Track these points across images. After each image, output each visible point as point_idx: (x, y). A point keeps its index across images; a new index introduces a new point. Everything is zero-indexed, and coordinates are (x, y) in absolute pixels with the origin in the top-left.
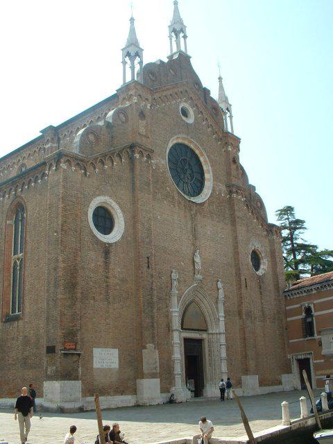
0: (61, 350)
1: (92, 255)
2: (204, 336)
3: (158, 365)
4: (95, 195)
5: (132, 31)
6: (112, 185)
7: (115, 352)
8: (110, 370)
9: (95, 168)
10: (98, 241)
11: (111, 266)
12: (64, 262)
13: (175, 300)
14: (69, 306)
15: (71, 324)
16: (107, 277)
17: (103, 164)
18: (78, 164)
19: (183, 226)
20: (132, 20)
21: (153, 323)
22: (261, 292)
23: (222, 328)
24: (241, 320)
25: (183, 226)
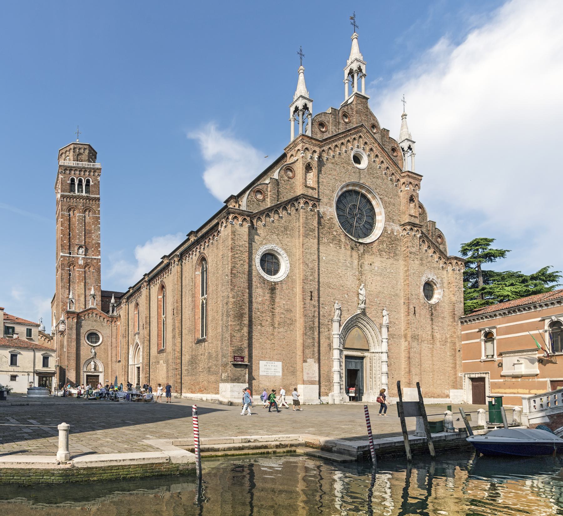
0: (232, 362)
1: (260, 291)
6: (278, 235)
10: (264, 280)
11: (277, 300)
12: (233, 297)
14: (238, 330)
15: (239, 343)
16: (273, 308)
19: (349, 265)
22: (432, 319)
24: (406, 342)
25: (349, 265)
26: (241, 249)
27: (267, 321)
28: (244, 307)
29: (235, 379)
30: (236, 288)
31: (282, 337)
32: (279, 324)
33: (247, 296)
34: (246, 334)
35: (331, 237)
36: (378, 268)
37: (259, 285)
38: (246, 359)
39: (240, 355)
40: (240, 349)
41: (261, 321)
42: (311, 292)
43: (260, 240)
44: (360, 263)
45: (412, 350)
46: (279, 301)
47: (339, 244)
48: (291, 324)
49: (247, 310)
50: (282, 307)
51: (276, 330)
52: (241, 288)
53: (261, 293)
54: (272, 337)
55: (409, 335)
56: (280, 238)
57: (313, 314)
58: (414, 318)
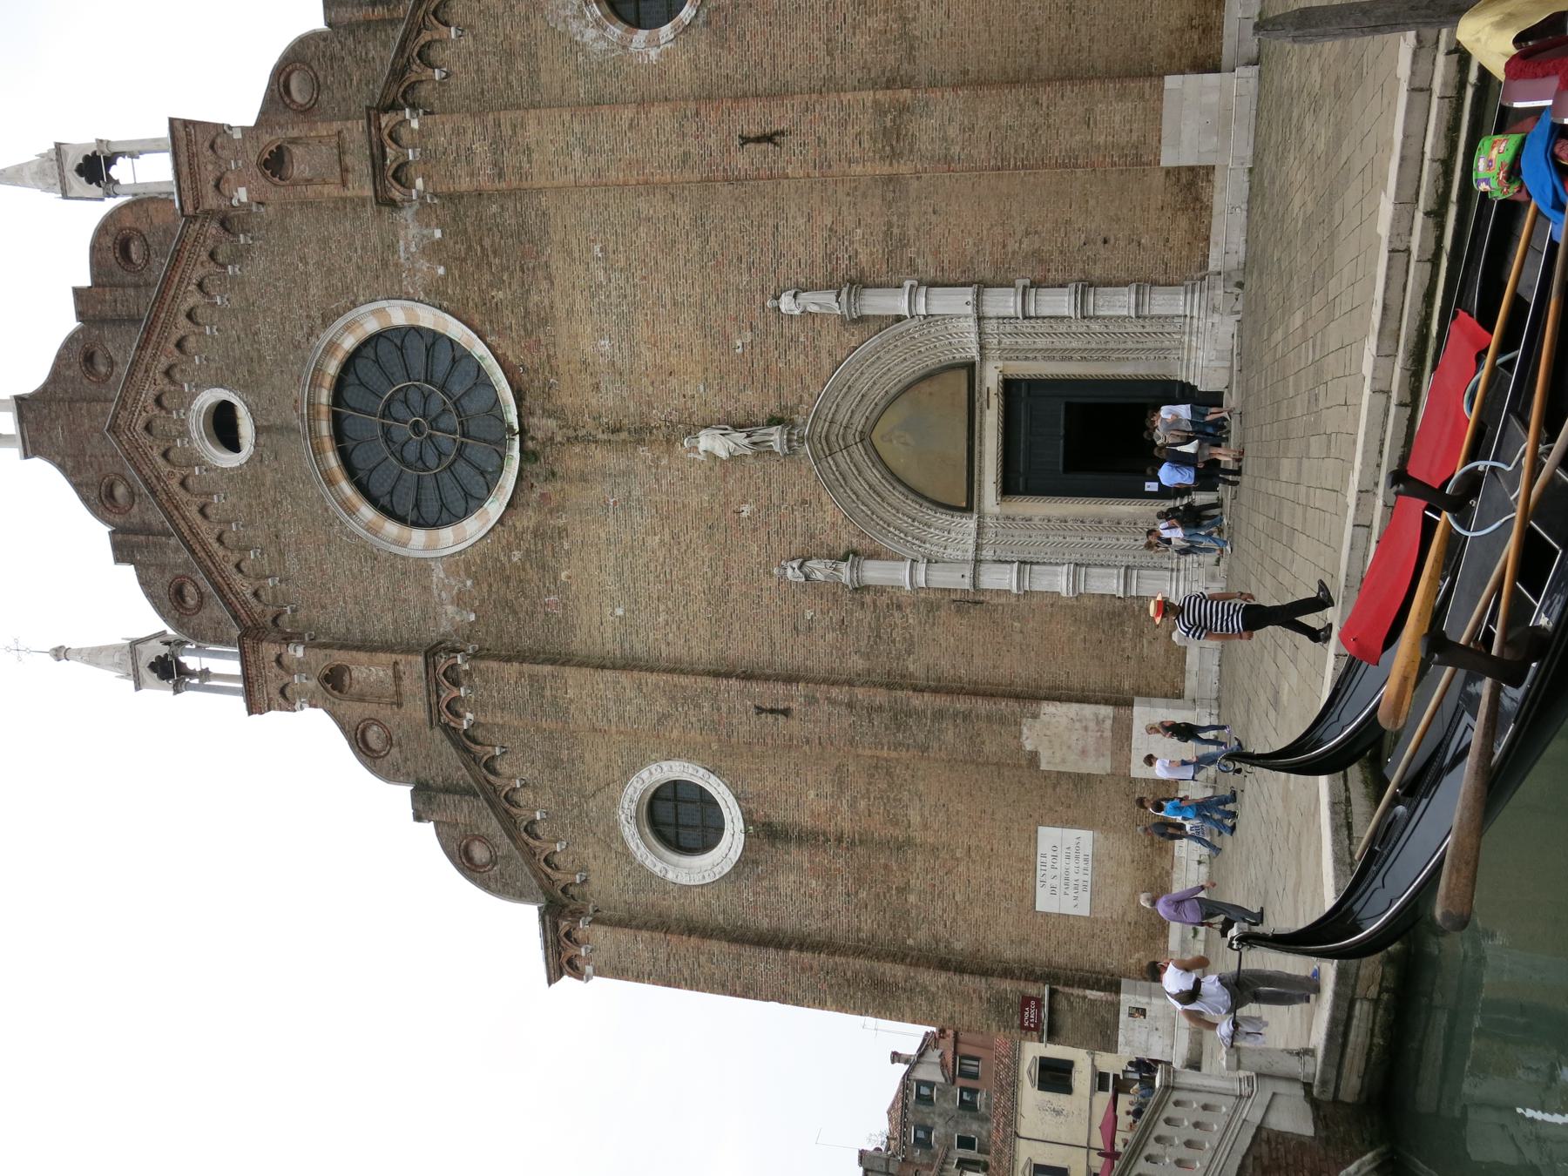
1: (786, 881)
2: (991, 379)
3: (1088, 710)
4: (627, 855)
5: (94, 656)
6: (584, 797)
7: (1050, 837)
8: (1096, 858)
9: (555, 852)
10: (746, 862)
11: (807, 821)
13: (874, 572)
15: (976, 1004)
16: (839, 840)
17: (533, 822)
18: (568, 935)
19: (620, 493)
20: (60, 653)
21: (956, 715)
23: (954, 303)
25: (620, 493)
26: (662, 956)
27: (886, 867)
28: (849, 974)
29: (1104, 1035)
30: (791, 989)
31: (942, 816)
32: (896, 824)
33: (810, 955)
34: (943, 977)
35: (532, 574)
36: (600, 332)
37: (765, 883)
38: (1032, 990)
39: (1017, 1009)
40: (998, 1004)
41: (889, 889)
42: (760, 710)
43: (615, 862)
44: (600, 436)
45: (955, 150)
46: (807, 812)
47: (552, 537)
48: (888, 773)
49: (860, 963)
50: (830, 802)
51: (918, 836)
52: (787, 975)
53: (792, 878)
54: (943, 854)
55: (885, 169)
56: (590, 787)
57: (844, 710)
58: (791, 142)
